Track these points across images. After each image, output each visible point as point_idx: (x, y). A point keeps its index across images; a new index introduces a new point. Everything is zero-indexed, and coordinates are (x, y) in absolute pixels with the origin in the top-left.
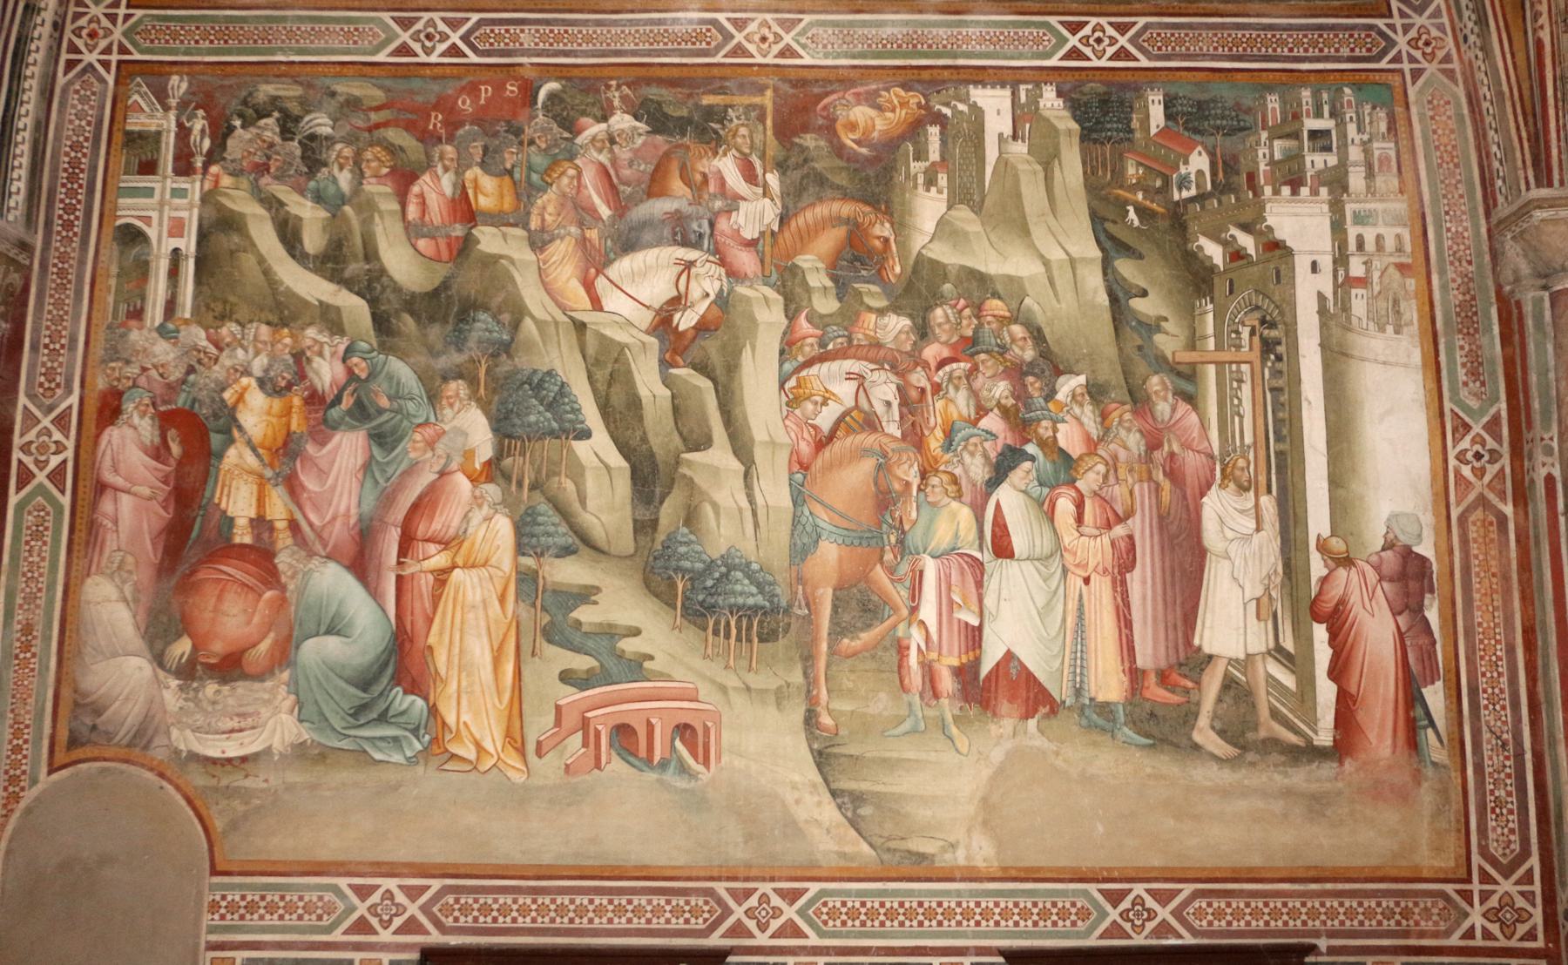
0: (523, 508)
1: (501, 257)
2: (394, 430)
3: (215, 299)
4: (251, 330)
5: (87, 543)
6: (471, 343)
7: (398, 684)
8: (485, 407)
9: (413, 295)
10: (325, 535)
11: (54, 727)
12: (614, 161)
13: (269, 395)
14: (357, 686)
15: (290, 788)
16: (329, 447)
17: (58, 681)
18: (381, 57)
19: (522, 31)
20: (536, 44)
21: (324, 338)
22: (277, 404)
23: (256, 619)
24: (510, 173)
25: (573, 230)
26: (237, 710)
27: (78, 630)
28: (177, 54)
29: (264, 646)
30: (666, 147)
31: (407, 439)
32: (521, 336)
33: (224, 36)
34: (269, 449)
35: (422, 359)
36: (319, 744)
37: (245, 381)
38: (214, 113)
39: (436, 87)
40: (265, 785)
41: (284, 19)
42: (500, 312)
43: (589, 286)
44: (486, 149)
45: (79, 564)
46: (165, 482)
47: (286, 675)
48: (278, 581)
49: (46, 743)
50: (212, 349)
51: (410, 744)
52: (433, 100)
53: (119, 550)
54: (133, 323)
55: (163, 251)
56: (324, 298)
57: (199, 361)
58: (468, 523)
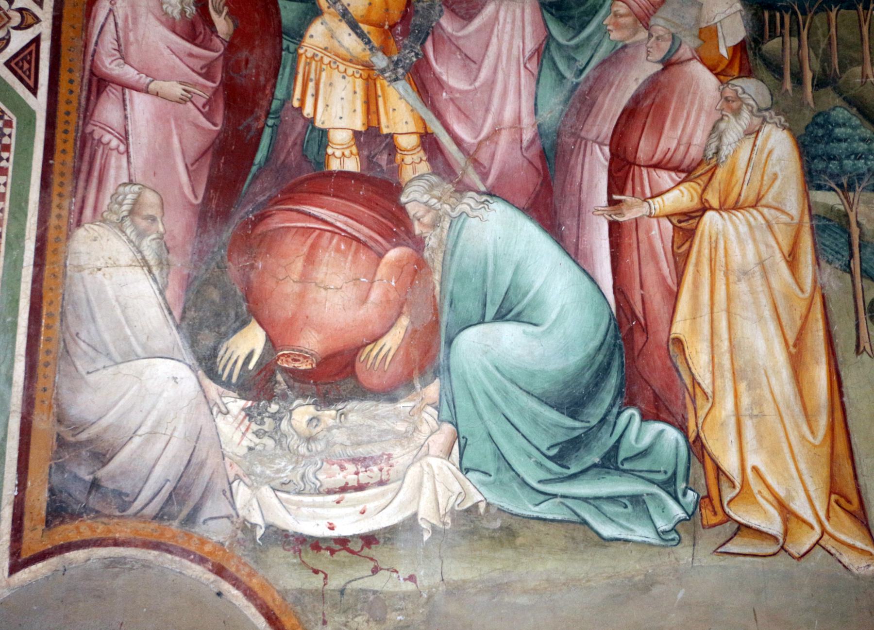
5: (77, 172)
7: (631, 403)
10: (483, 157)
11: (22, 485)
14: (558, 407)
15: (455, 590)
16: (477, 22)
17: (29, 402)
23: (376, 294)
26: (350, 451)
27: (63, 314)
29: (392, 341)
31: (603, 12)
34: (379, 25)
36: (500, 510)
40: (410, 586)
47: (433, 390)
48: (409, 231)
51: (664, 509)
53: (131, 182)
58: (720, 139)
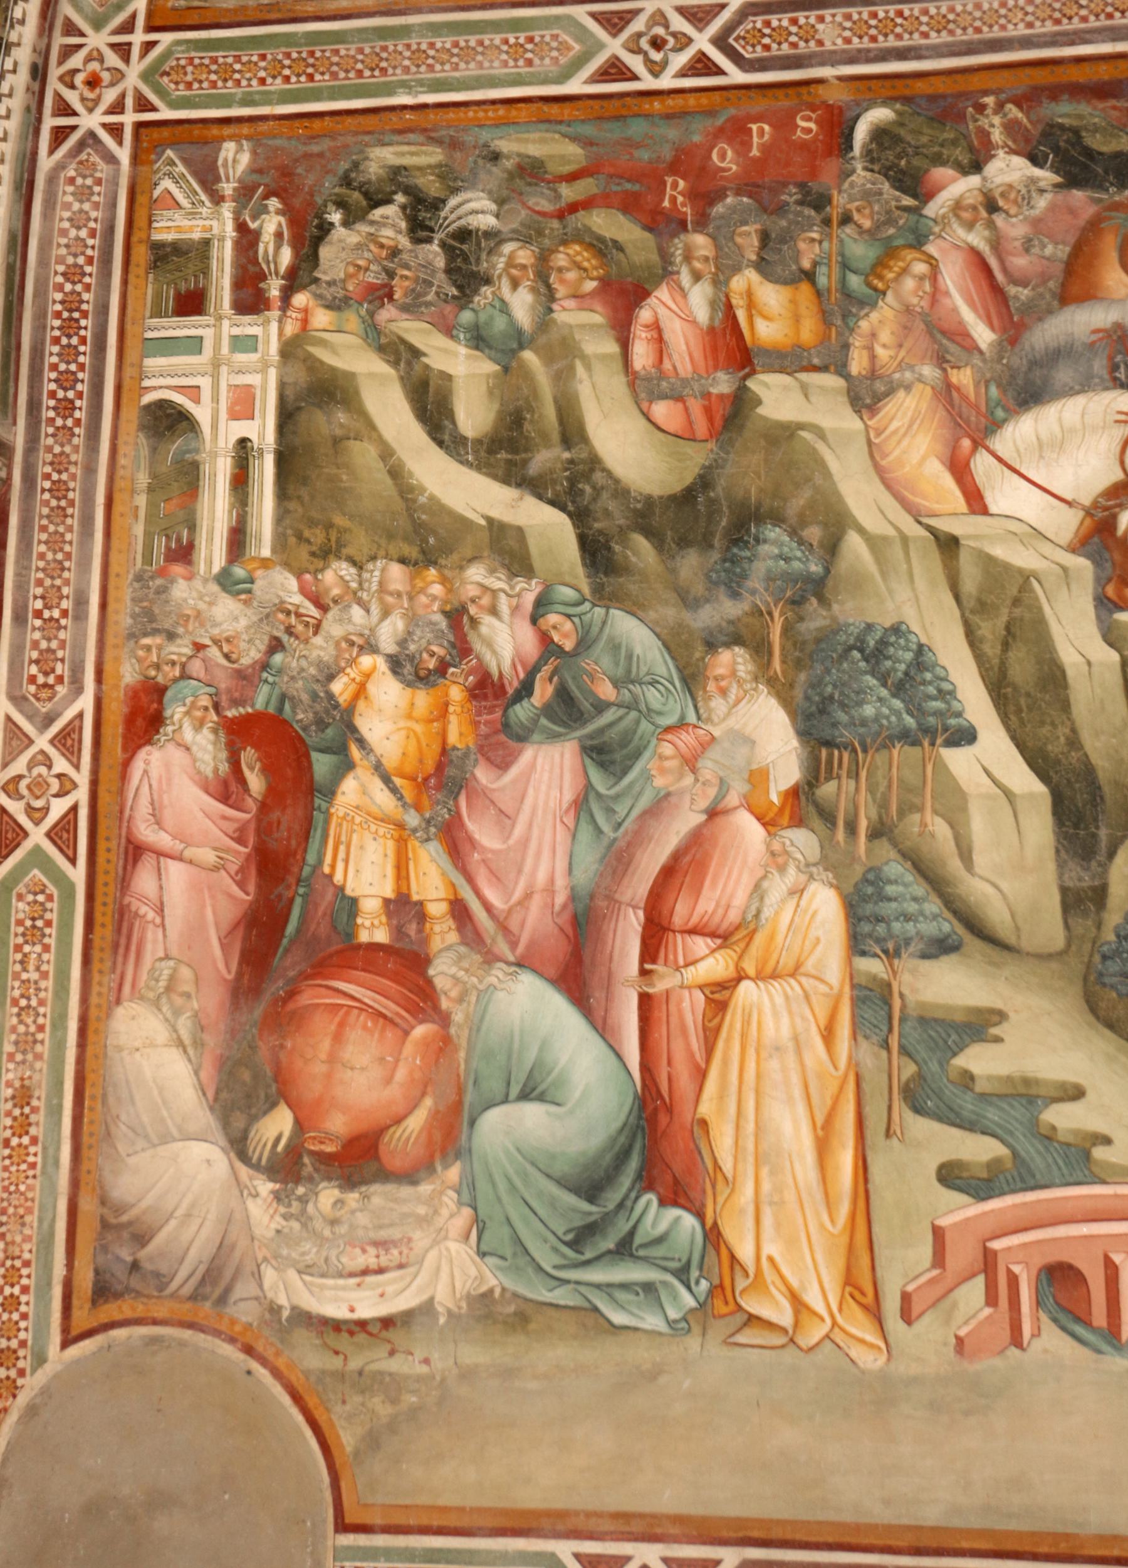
0: (858, 870)
1: (801, 426)
2: (625, 740)
3: (312, 523)
4: (375, 572)
5: (116, 946)
6: (755, 582)
7: (650, 1187)
8: (783, 693)
9: (649, 501)
10: (514, 924)
11: (70, 1265)
12: (996, 244)
13: (409, 684)
14: (576, 1191)
15: (467, 1374)
16: (514, 771)
17: (75, 1184)
18: (575, 86)
19: (821, 19)
20: (848, 41)
21: (498, 582)
22: (423, 699)
23: (401, 1074)
24: (809, 276)
25: (929, 371)
26: (372, 1235)
27: (104, 1096)
28: (229, 106)
29: (416, 1122)
30: (1091, 211)
31: (647, 754)
32: (843, 565)
33: (306, 67)
34: (413, 779)
35: (670, 613)
36: (516, 1295)
37: (366, 661)
38: (297, 202)
39: (672, 133)
40: (424, 1369)
41: (406, 30)
42: (803, 522)
43: (960, 470)
44: (765, 237)
45: (103, 983)
46: (240, 840)
47: (453, 1173)
48: (436, 1007)
49: (57, 1292)
50: (313, 611)
51: (675, 1297)
52: (667, 154)
53: (167, 957)
54: (177, 569)
55: (221, 443)
56: (495, 514)
57: (289, 630)
58: (762, 899)
